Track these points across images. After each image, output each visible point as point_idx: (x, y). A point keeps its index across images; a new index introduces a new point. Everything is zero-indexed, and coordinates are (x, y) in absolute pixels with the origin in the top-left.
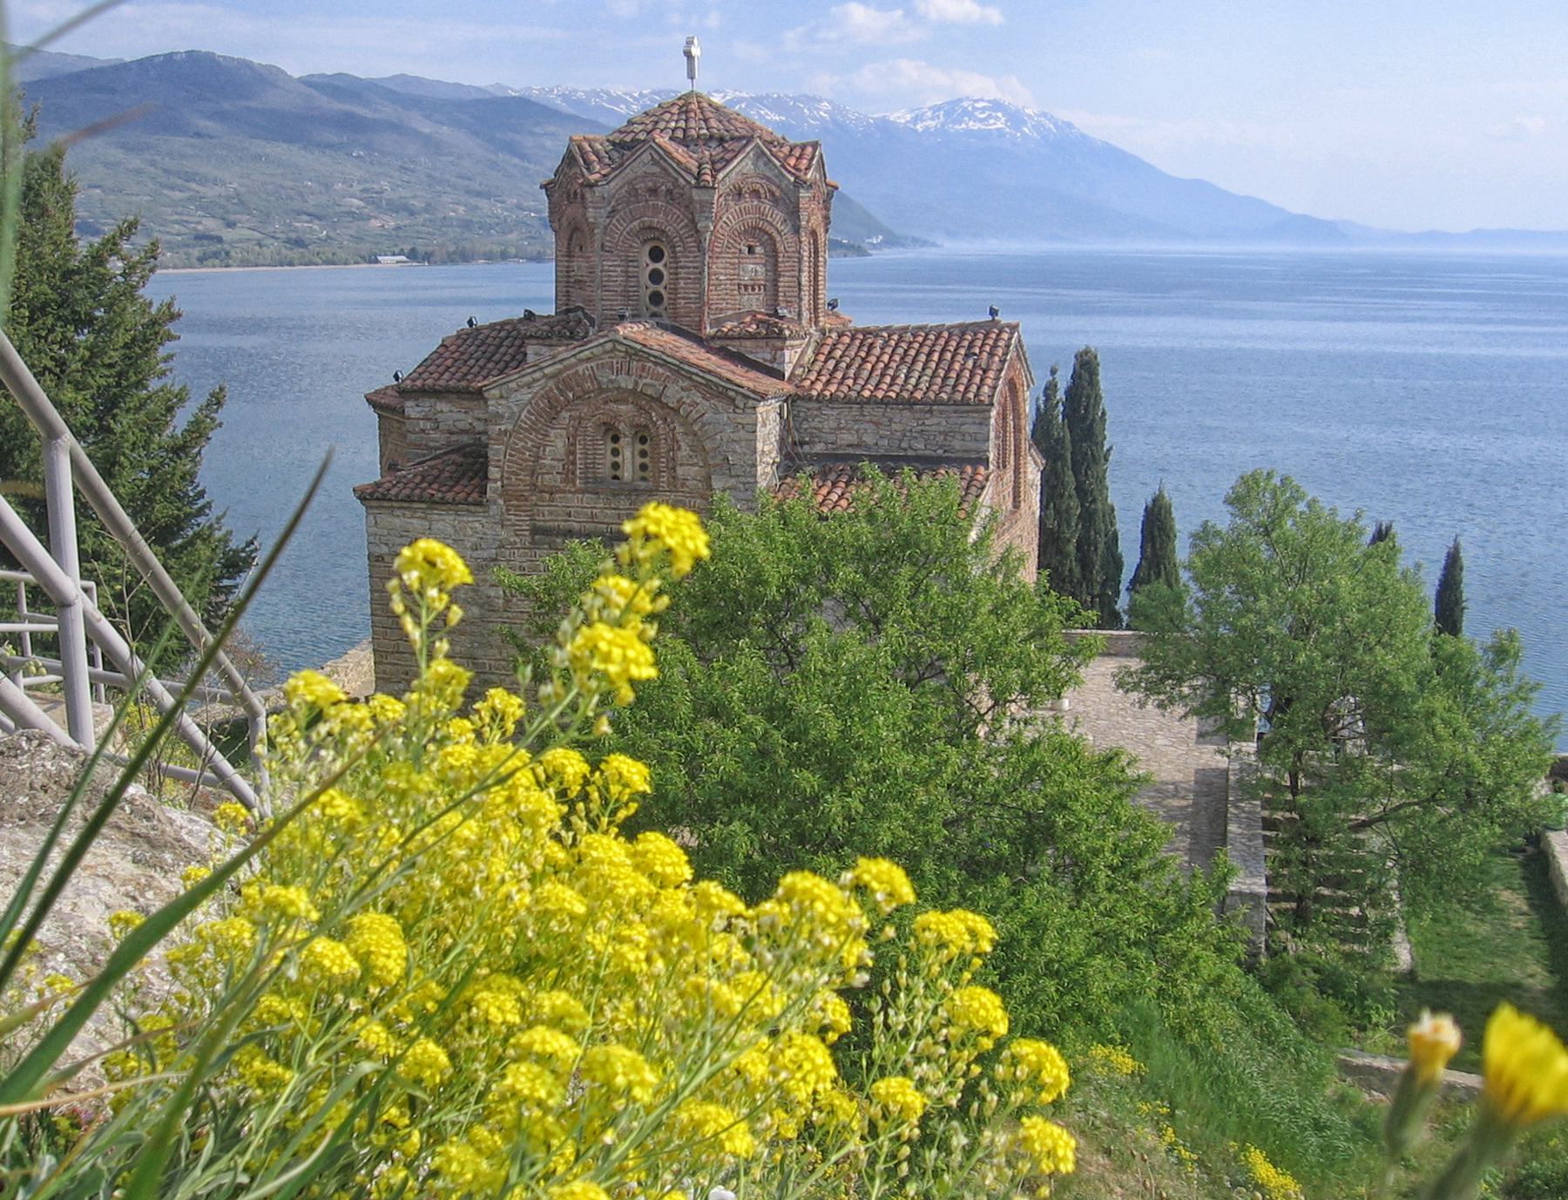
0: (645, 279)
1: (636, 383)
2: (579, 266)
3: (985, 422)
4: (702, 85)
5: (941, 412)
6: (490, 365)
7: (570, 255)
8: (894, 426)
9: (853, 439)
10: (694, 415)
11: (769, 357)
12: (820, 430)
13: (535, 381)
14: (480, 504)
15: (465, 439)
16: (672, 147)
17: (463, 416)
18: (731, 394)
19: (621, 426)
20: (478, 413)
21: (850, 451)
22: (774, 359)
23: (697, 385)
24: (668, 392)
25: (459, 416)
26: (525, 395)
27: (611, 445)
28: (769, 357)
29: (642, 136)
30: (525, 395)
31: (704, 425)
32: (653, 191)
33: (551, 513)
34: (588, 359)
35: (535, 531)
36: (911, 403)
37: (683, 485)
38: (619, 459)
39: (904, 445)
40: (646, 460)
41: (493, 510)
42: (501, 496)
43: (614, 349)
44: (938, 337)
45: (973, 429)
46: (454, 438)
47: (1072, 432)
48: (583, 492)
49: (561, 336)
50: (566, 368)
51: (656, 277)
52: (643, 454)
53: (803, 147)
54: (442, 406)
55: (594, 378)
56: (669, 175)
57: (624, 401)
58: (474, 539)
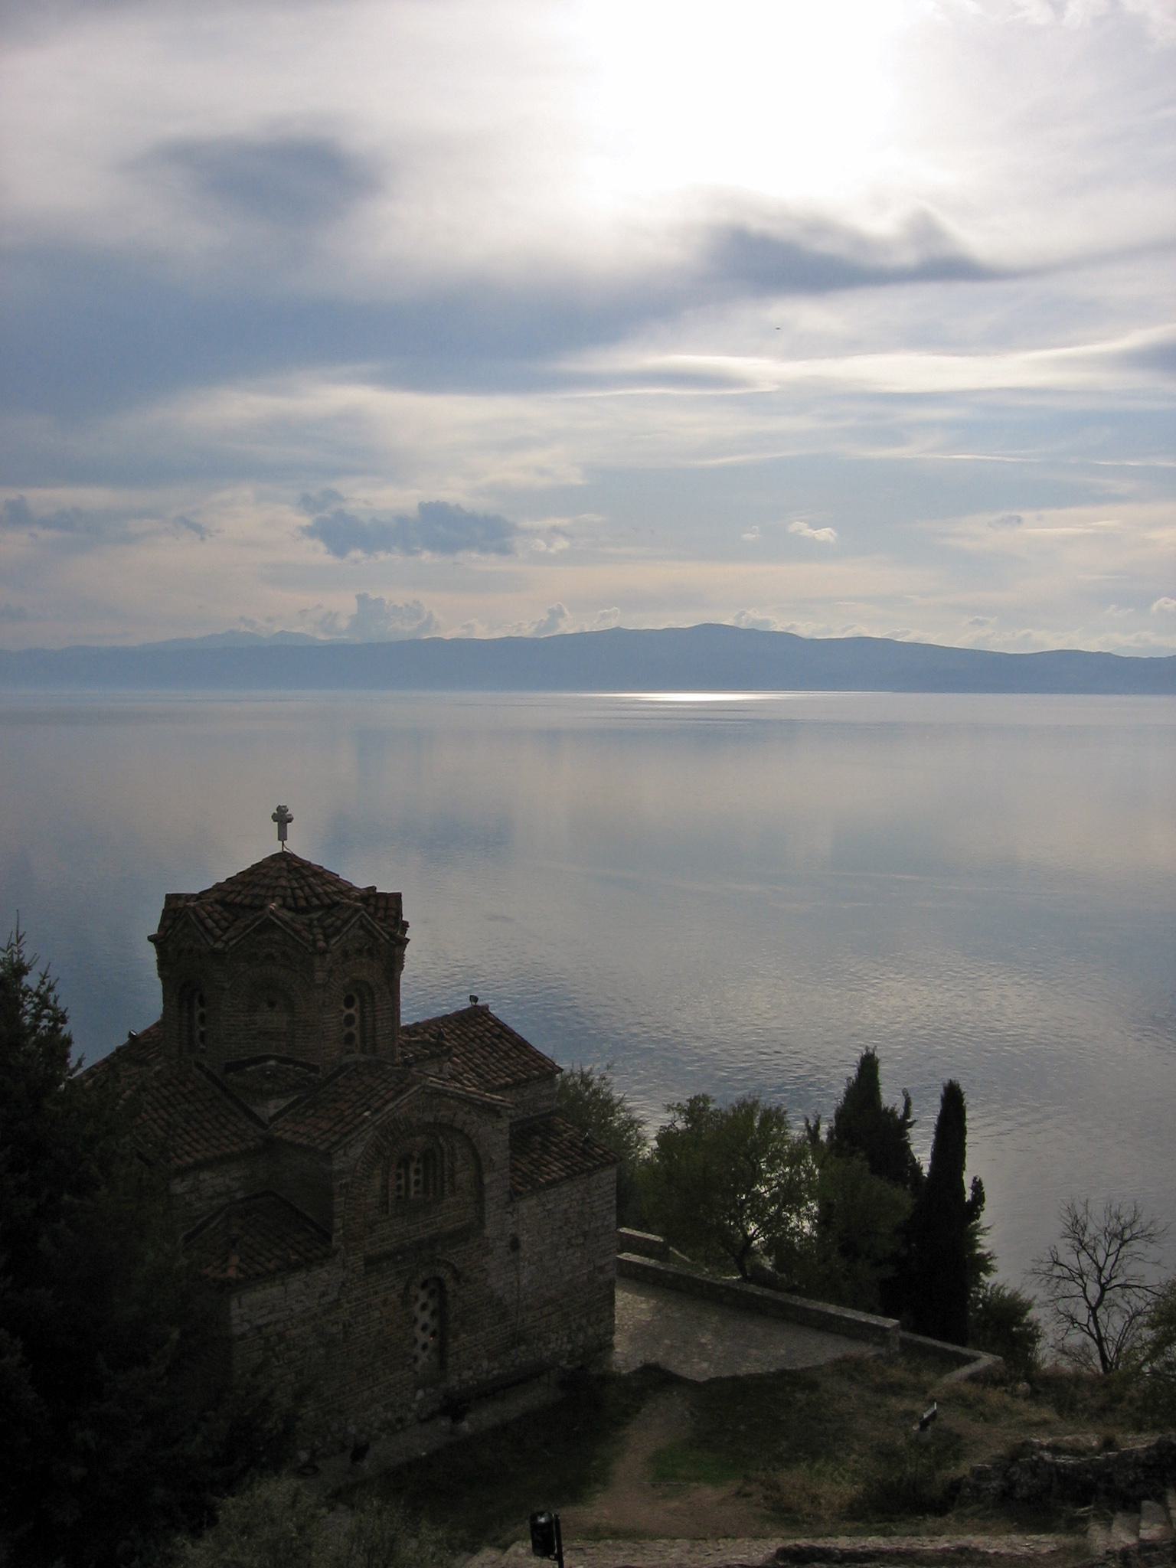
19: (416, 1154)
22: (441, 1071)
26: (358, 1150)
30: (358, 1150)
35: (371, 1262)
38: (402, 1181)
51: (349, 1020)
52: (417, 1172)
54: (205, 1175)
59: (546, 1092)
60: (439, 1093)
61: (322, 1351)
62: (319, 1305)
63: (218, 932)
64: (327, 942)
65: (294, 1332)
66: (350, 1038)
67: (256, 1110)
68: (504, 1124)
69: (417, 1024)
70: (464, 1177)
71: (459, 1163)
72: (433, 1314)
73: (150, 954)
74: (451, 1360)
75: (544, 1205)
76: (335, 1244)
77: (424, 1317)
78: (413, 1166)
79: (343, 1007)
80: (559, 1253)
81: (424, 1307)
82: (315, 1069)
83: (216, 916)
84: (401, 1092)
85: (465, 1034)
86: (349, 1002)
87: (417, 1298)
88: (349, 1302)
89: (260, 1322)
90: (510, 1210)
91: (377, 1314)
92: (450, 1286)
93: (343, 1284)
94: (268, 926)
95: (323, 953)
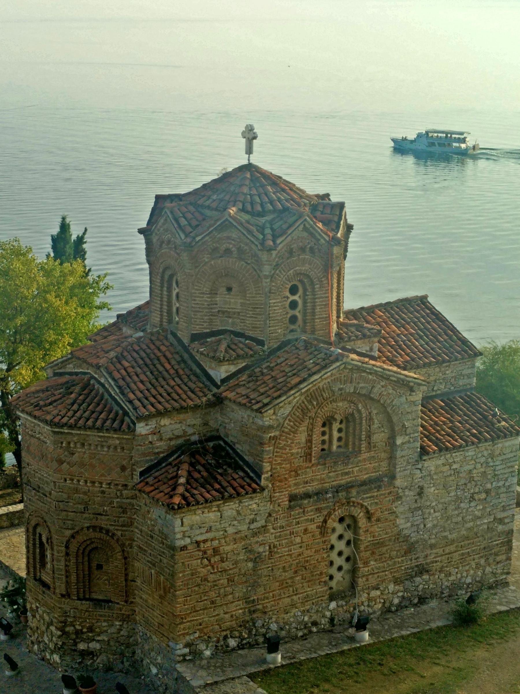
4: (255, 160)
5: (454, 365)
7: (213, 292)
10: (389, 401)
15: (180, 441)
18: (412, 384)
19: (338, 417)
22: (371, 349)
24: (375, 390)
25: (173, 427)
26: (287, 410)
28: (368, 348)
32: (303, 249)
34: (326, 379)
35: (293, 498)
37: (374, 447)
38: (326, 437)
43: (345, 368)
48: (318, 464)
51: (293, 305)
52: (340, 430)
54: (165, 421)
57: (343, 400)
58: (252, 517)
59: (466, 372)
60: (359, 369)
61: (250, 565)
62: (249, 528)
63: (189, 229)
64: (274, 241)
65: (227, 548)
66: (293, 320)
67: (212, 373)
68: (418, 397)
69: (362, 308)
70: (379, 437)
71: (376, 426)
72: (348, 543)
73: (141, 242)
74: (361, 581)
75: (450, 465)
76: (263, 483)
77: (340, 546)
78: (336, 426)
79: (288, 294)
80: (462, 505)
81: (341, 537)
82: (261, 343)
83: (189, 216)
84: (325, 367)
85: (403, 319)
86: (293, 290)
87: (334, 530)
88: (274, 529)
89: (200, 538)
90: (420, 466)
91: (298, 540)
92: (362, 522)
93: (270, 515)
94: (226, 225)
95: (270, 250)
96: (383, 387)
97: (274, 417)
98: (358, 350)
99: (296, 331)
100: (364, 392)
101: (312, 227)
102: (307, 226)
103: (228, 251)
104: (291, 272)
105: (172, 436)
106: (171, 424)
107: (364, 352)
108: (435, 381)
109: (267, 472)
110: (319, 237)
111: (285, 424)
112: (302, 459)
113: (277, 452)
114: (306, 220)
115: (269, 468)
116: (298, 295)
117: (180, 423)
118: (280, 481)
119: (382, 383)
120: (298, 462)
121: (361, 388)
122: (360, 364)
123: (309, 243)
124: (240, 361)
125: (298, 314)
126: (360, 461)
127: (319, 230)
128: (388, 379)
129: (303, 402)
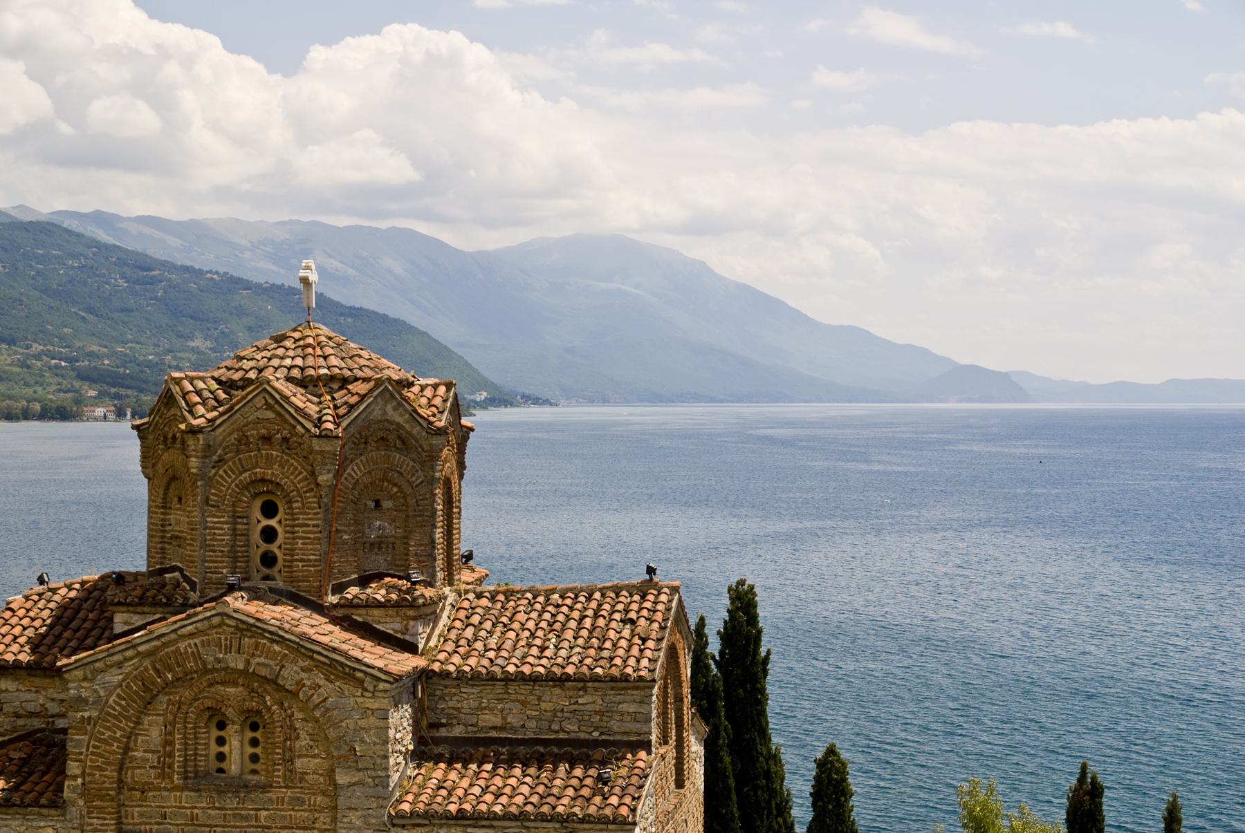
0: (256, 536)
1: (248, 663)
2: (179, 520)
3: (645, 701)
6: (67, 634)
7: (165, 506)
8: (543, 706)
9: (498, 721)
11: (398, 626)
12: (458, 710)
13: (126, 660)
14: (53, 805)
15: (37, 723)
16: (287, 389)
17: (33, 696)
18: (359, 675)
19: (230, 713)
20: (52, 693)
21: (494, 734)
22: (406, 630)
23: (319, 665)
24: (285, 673)
25: (28, 696)
26: (114, 677)
27: (215, 733)
29: (252, 375)
30: (114, 677)
31: (327, 710)
32: (267, 439)
33: (141, 815)
34: (191, 635)
36: (563, 680)
38: (225, 749)
39: (555, 727)
40: (258, 750)
41: (73, 812)
42: (81, 795)
44: (589, 598)
45: (632, 708)
46: (21, 722)
47: (730, 679)
49: (156, 604)
50: (165, 645)
51: (269, 535)
52: (254, 742)
53: (435, 386)
55: (197, 656)
56: (286, 421)
57: (235, 684)
76: (67, 794)
79: (257, 514)
86: (269, 510)
96: (303, 669)
97: (85, 684)
98: (378, 627)
99: (274, 579)
100: (264, 672)
101: (277, 402)
102: (270, 401)
103: (174, 437)
104: (246, 474)
105: (22, 712)
106: (18, 690)
107: (391, 632)
108: (554, 713)
109: (75, 778)
110: (292, 422)
111: (111, 701)
112: (152, 771)
113: (94, 747)
114: (265, 390)
115: (78, 772)
116: (277, 518)
117: (37, 692)
118: (102, 798)
119: (301, 663)
120: (139, 775)
121: (259, 664)
122: (251, 621)
123: (278, 431)
124: (146, 609)
125: (277, 551)
126: (270, 800)
127: (292, 411)
128: (312, 658)
129: (146, 670)
